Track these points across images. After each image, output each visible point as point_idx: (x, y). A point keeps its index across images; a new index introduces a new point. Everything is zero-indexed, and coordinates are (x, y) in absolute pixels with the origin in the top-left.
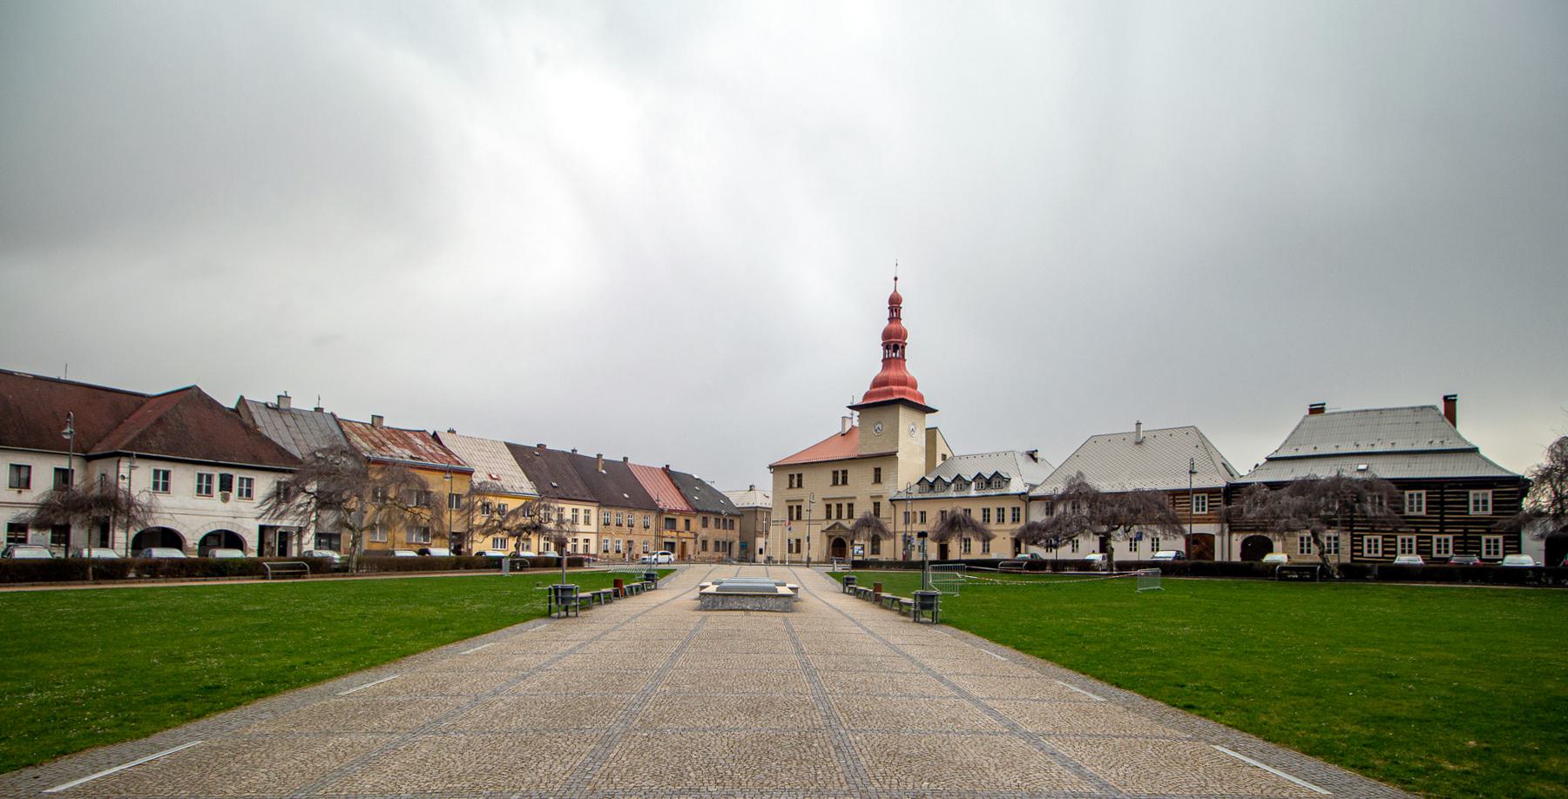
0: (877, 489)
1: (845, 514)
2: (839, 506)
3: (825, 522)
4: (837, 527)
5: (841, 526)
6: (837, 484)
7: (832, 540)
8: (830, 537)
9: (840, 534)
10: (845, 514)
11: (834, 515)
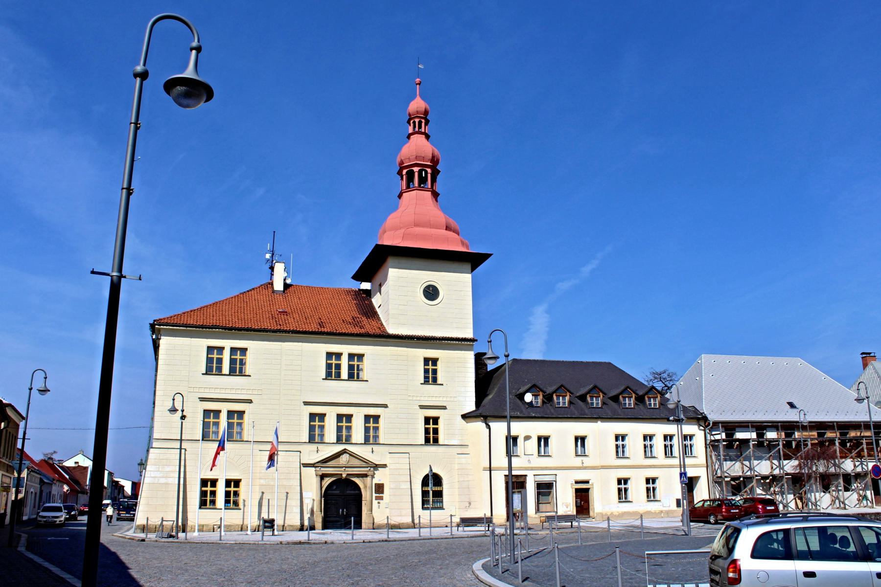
0: (431, 395)
1: (358, 433)
2: (344, 419)
3: (313, 447)
4: (344, 458)
5: (352, 455)
6: (338, 376)
7: (327, 481)
8: (323, 477)
9: (343, 468)
10: (358, 433)
11: (330, 434)
